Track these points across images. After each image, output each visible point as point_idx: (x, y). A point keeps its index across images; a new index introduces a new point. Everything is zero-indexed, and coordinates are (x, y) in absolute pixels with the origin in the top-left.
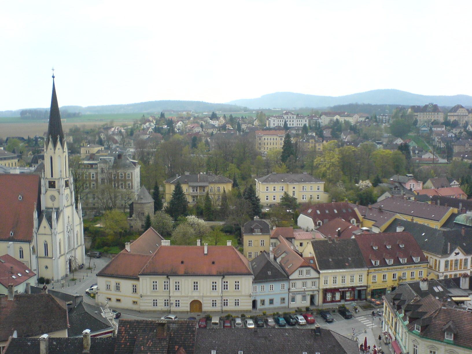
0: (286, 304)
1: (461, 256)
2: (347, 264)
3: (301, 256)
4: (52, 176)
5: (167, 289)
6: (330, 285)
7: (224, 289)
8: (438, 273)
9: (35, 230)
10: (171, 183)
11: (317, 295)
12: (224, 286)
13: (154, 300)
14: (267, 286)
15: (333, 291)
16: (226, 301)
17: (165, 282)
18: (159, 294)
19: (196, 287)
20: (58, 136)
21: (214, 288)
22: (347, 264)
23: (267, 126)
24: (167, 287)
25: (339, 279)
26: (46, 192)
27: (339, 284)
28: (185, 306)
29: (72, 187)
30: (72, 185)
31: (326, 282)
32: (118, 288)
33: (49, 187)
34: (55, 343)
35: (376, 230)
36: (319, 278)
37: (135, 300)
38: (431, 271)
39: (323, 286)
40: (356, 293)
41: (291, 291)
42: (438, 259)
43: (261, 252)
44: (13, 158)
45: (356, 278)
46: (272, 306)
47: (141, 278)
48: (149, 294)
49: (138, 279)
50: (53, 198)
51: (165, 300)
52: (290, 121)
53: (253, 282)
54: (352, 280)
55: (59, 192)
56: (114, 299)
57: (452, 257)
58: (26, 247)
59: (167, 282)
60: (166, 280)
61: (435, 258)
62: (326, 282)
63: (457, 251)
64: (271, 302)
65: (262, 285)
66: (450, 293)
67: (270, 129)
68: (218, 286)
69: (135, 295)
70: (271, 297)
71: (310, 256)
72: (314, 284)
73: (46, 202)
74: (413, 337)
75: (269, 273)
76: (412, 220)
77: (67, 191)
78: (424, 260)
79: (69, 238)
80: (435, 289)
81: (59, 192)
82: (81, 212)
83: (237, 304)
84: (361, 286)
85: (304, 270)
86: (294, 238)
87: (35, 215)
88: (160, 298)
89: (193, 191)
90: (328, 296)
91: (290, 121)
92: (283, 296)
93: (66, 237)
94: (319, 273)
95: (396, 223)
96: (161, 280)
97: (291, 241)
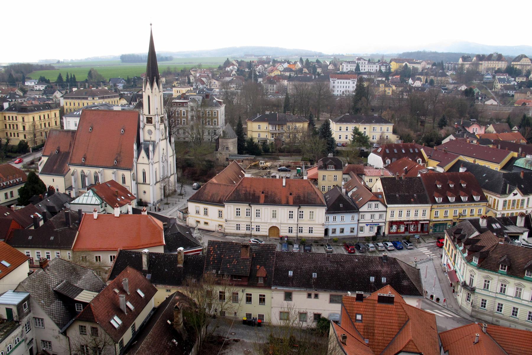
0: (355, 234)
1: (519, 197)
2: (412, 200)
3: (371, 191)
4: (149, 113)
5: (249, 215)
6: (396, 218)
7: (300, 217)
8: (496, 211)
9: (135, 160)
10: (253, 121)
11: (384, 227)
12: (300, 215)
13: (237, 225)
14: (339, 217)
15: (399, 223)
16: (301, 229)
17: (247, 210)
18: (242, 220)
19: (274, 216)
20: (155, 78)
21: (291, 216)
22: (412, 200)
23: (341, 70)
24: (248, 214)
25: (404, 213)
26: (144, 126)
27: (404, 218)
28: (264, 231)
29: (166, 122)
30: (166, 120)
31: (392, 215)
32: (206, 213)
34: (154, 257)
35: (440, 170)
36: (386, 211)
37: (221, 224)
38: (490, 209)
39: (389, 219)
40: (419, 226)
41: (360, 221)
42: (497, 199)
43: (334, 186)
44: (115, 97)
45: (420, 213)
46: (342, 235)
47: (226, 205)
48: (232, 219)
49: (224, 206)
50: (150, 132)
51: (247, 225)
52: (362, 66)
53: (326, 213)
54: (416, 215)
55: (155, 127)
56: (202, 222)
57: (511, 197)
58: (128, 174)
59: (249, 210)
60: (249, 208)
61: (494, 197)
62: (392, 215)
63: (515, 191)
64: (342, 231)
65: (335, 215)
66: (506, 229)
67: (343, 73)
68: (295, 215)
69: (220, 219)
70: (342, 227)
71: (379, 191)
72: (380, 216)
73: (144, 136)
74: (470, 268)
75: (341, 205)
76: (475, 161)
77: (162, 126)
78: (484, 199)
79: (163, 167)
80: (494, 225)
81: (155, 127)
82: (173, 145)
83: (311, 231)
84: (424, 220)
85: (373, 203)
86: (364, 174)
87: (135, 147)
88: (242, 223)
89: (273, 128)
90: (394, 228)
91: (362, 66)
92: (352, 226)
93: (161, 166)
94: (386, 207)
95: (459, 164)
96: (243, 208)
97: (361, 176)
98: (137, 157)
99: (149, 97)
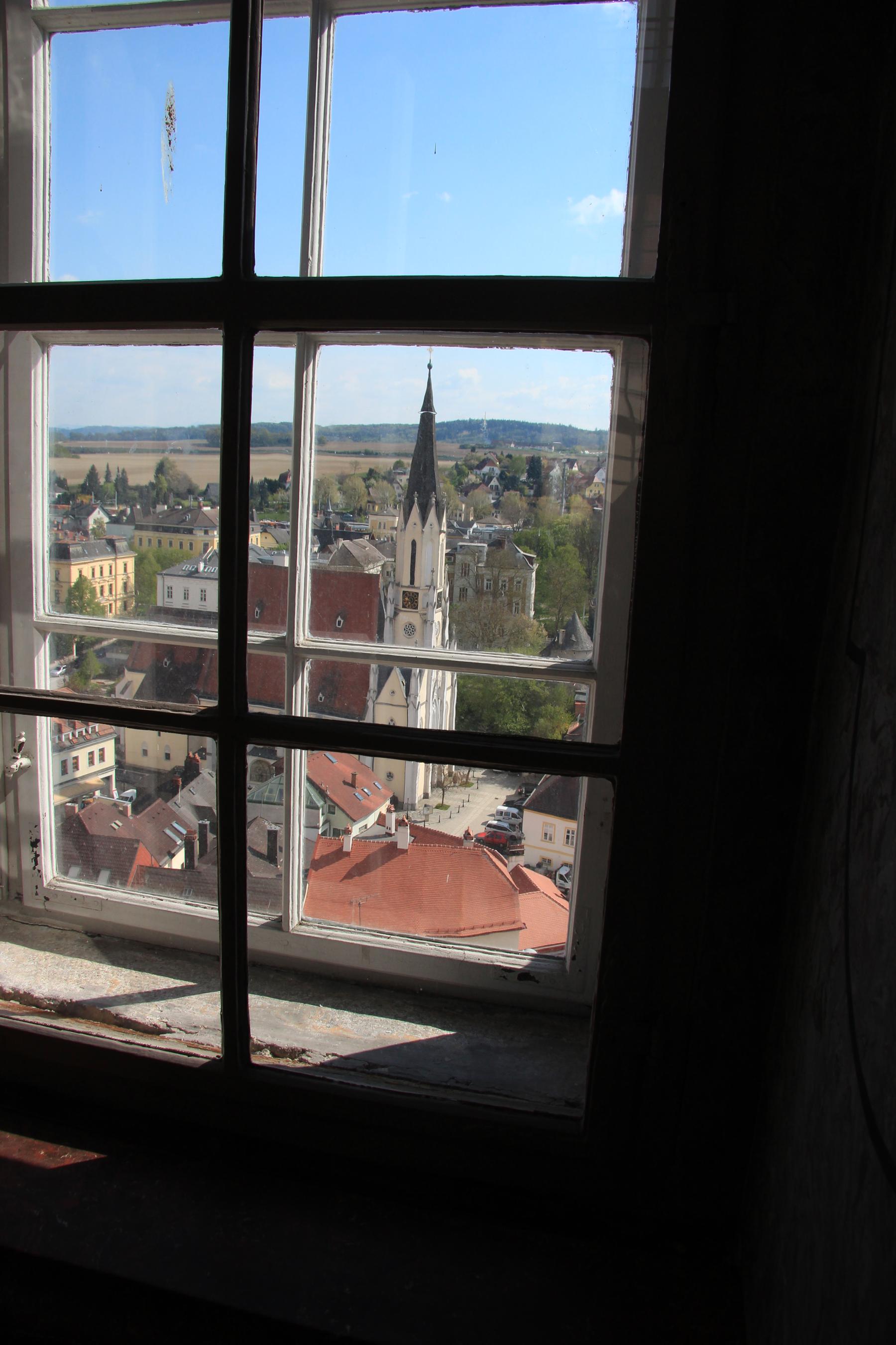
9: (371, 695)
26: (396, 614)
33: (404, 607)
98: (376, 689)
99: (414, 544)
